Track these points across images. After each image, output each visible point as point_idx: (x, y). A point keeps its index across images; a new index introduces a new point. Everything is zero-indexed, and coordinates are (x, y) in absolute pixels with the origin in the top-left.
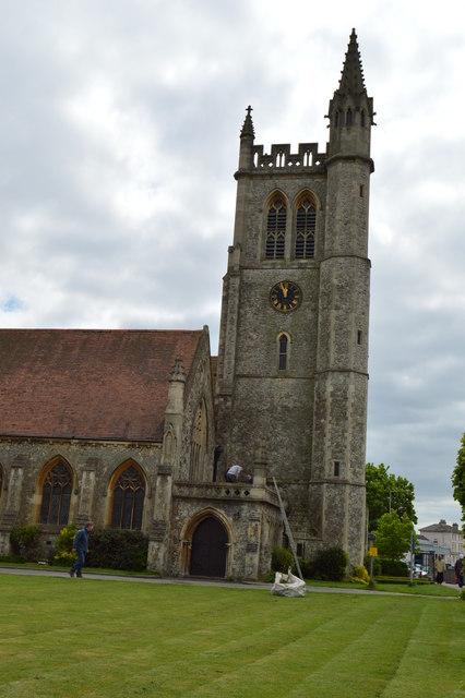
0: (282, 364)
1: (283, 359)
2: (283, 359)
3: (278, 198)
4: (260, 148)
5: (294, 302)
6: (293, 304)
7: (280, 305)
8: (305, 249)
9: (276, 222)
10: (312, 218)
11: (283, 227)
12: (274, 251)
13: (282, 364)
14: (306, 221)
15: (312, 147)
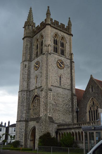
0: (60, 85)
1: (60, 82)
2: (60, 82)
3: (56, 35)
4: (51, 20)
5: (63, 67)
6: (63, 67)
7: (59, 67)
8: (63, 53)
9: (55, 42)
10: (63, 44)
11: (56, 44)
12: (56, 50)
13: (60, 85)
14: (62, 45)
15: (63, 25)
